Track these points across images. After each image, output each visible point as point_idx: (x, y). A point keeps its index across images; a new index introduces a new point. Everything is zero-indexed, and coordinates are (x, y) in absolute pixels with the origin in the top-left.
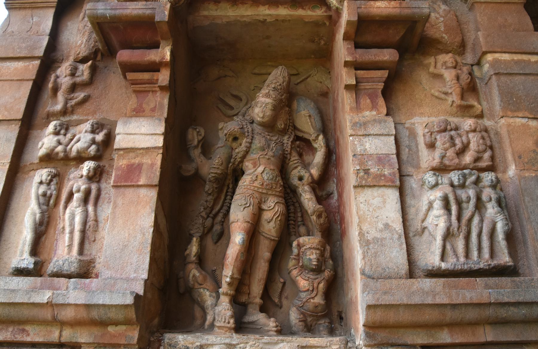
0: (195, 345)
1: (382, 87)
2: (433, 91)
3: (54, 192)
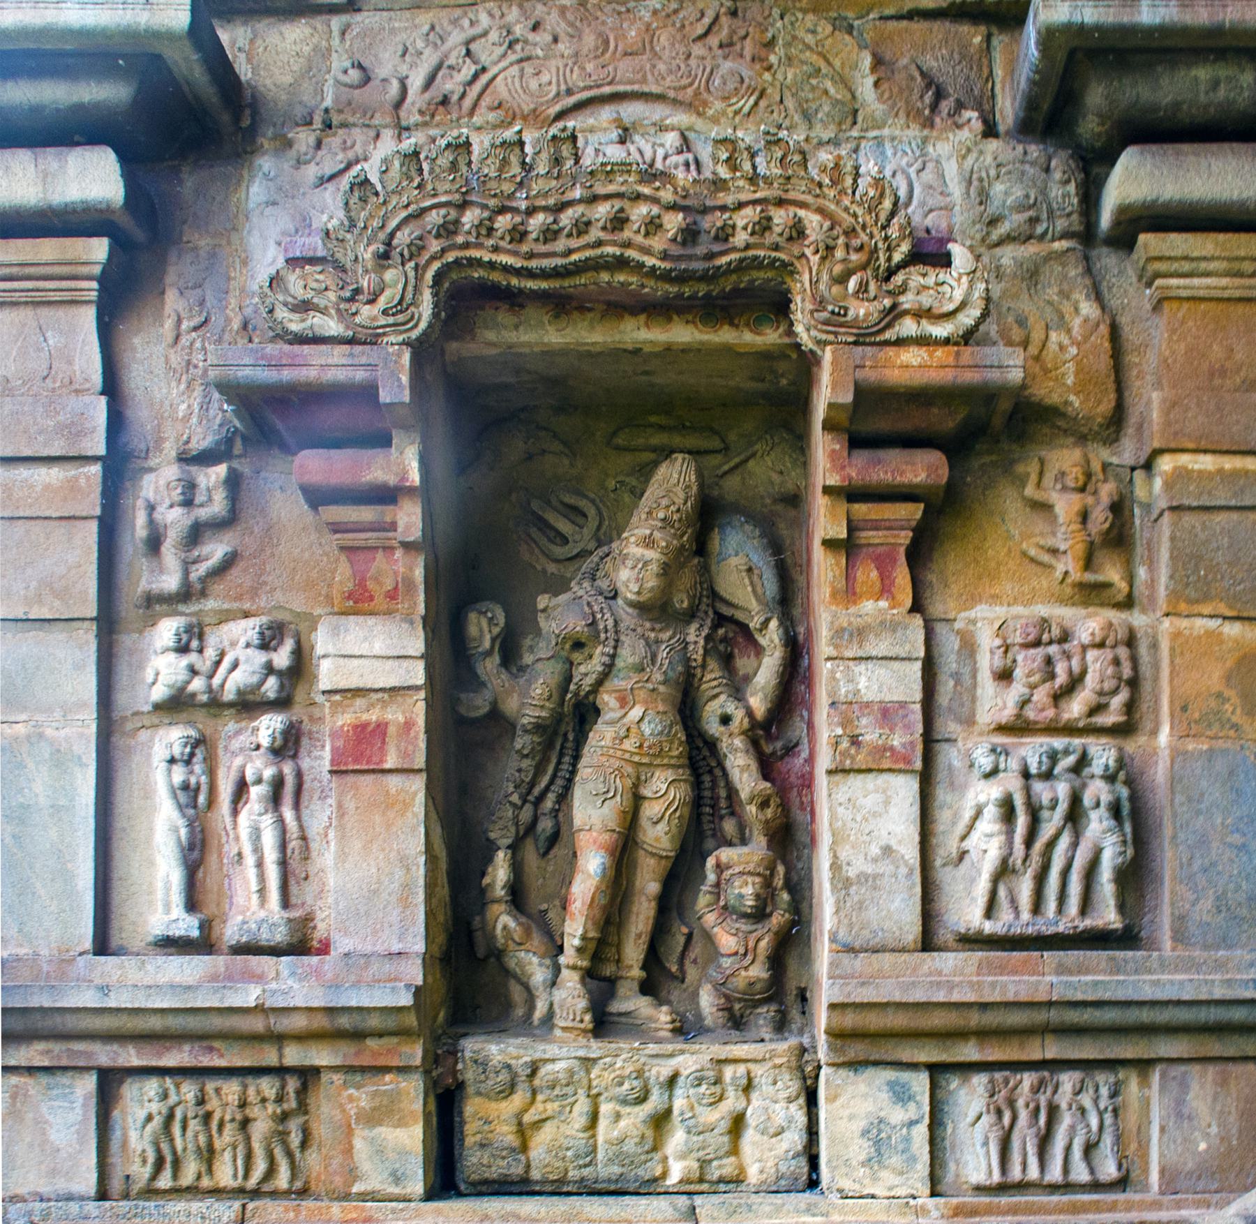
0: (521, 1061)
1: (908, 542)
2: (1024, 546)
3: (203, 779)
